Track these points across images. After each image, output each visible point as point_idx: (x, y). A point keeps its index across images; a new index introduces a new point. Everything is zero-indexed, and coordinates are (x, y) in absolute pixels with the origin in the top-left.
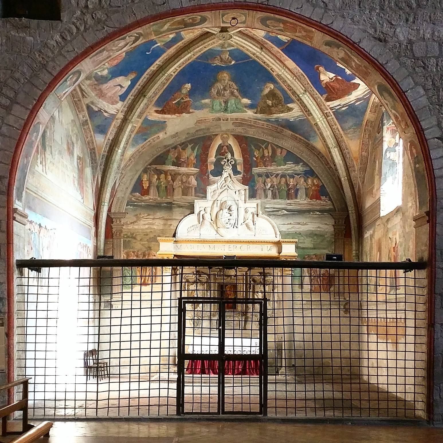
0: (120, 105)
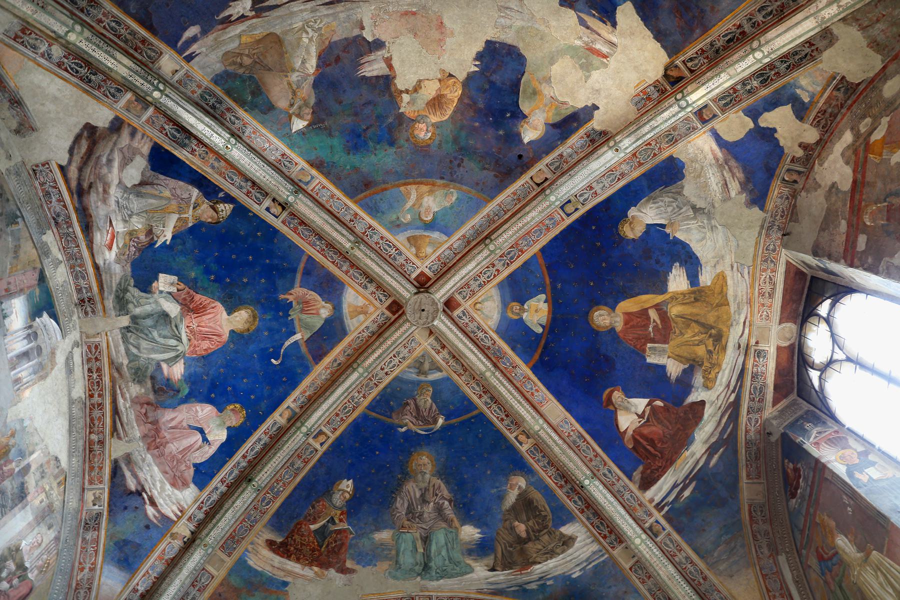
0: (189, 495)
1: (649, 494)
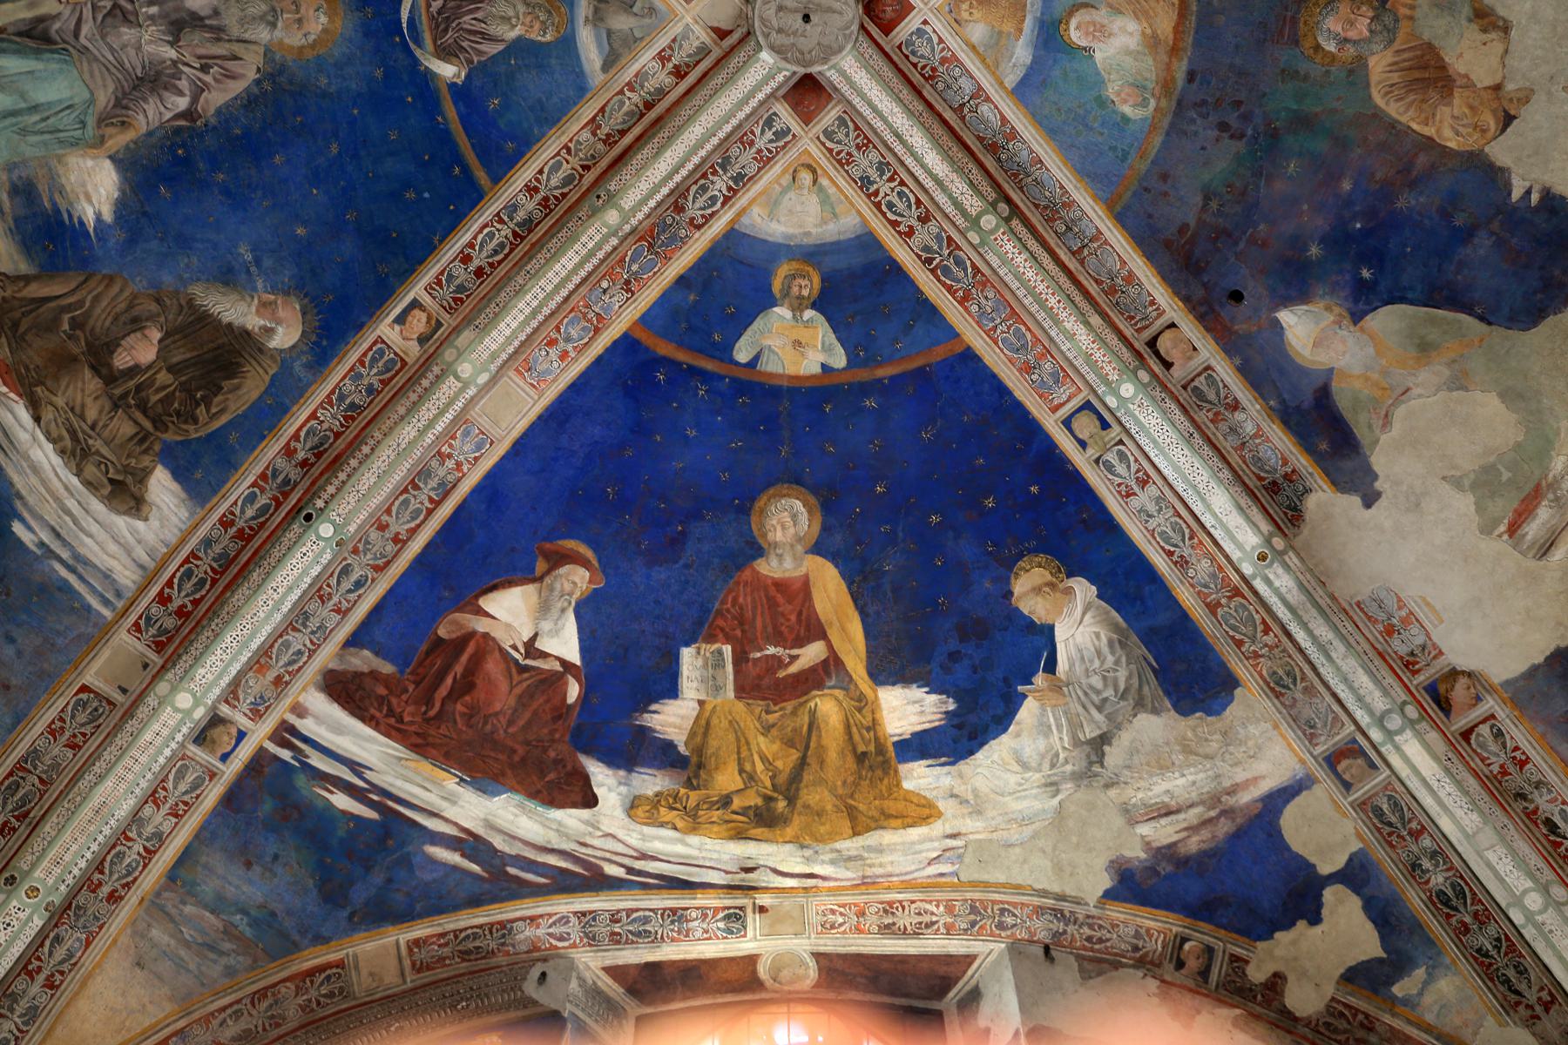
1: (318, 702)
